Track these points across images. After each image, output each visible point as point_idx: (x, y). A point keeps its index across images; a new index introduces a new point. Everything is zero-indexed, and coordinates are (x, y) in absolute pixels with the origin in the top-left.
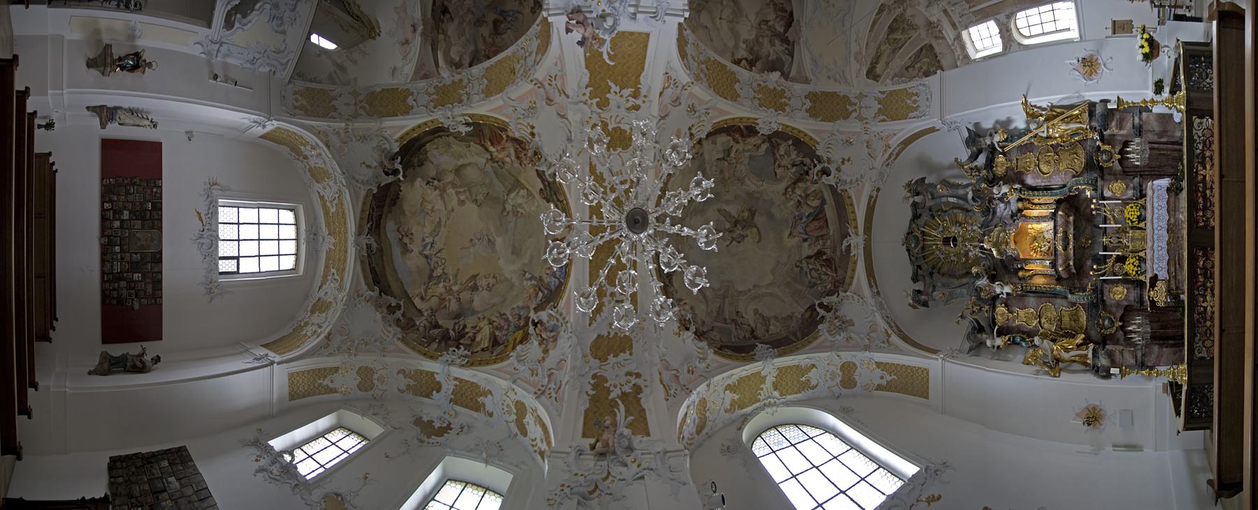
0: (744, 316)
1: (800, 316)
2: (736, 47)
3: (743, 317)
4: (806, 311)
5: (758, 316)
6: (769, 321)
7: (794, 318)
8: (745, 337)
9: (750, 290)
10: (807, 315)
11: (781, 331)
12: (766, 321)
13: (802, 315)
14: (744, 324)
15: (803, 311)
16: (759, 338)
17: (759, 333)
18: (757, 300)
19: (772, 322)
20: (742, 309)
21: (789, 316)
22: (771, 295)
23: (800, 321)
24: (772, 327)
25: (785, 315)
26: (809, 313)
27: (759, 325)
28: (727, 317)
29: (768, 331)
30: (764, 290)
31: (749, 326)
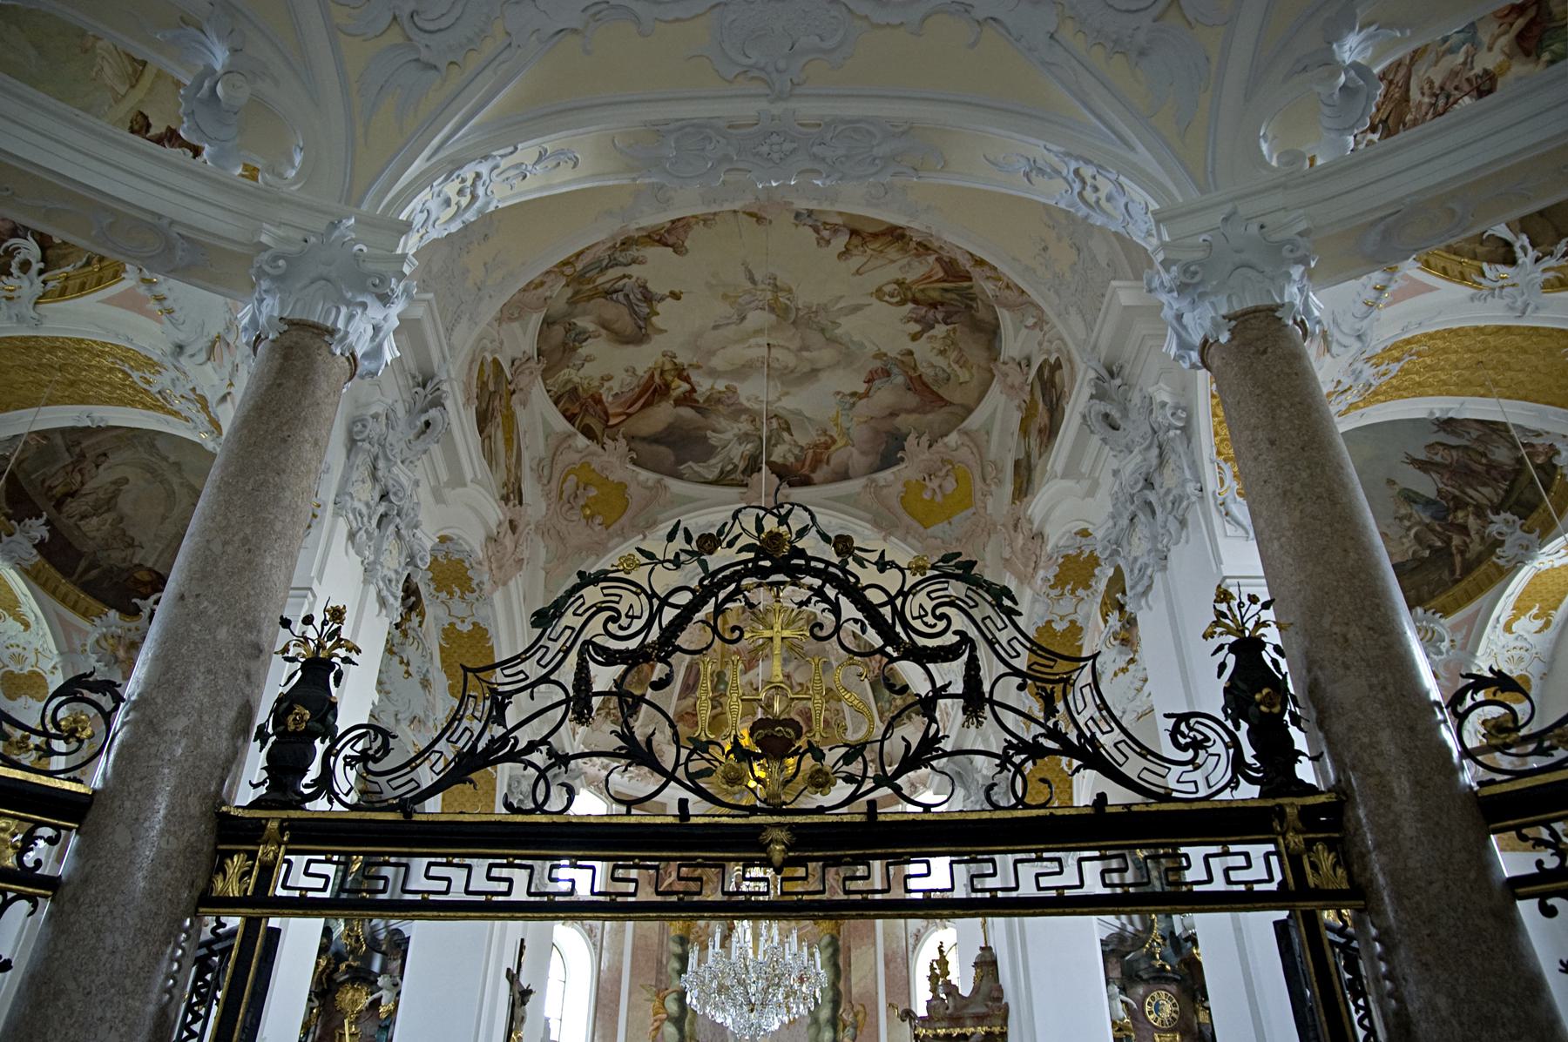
0: (101, 468)
1: (136, 561)
2: (713, 373)
3: (97, 466)
4: (150, 570)
5: (113, 488)
6: (109, 510)
7: (130, 551)
8: (50, 488)
9: (165, 459)
10: (143, 576)
11: (93, 539)
12: (109, 503)
13: (140, 565)
14: (82, 475)
15: (149, 565)
16: (60, 512)
17: (72, 506)
18: (148, 475)
19: (110, 517)
20: (114, 458)
21: (133, 539)
22: (171, 494)
23: (123, 565)
24: (94, 521)
25: (131, 532)
26: (147, 578)
27: (91, 498)
28: (85, 444)
29: (83, 517)
30: (175, 481)
31: (83, 484)
